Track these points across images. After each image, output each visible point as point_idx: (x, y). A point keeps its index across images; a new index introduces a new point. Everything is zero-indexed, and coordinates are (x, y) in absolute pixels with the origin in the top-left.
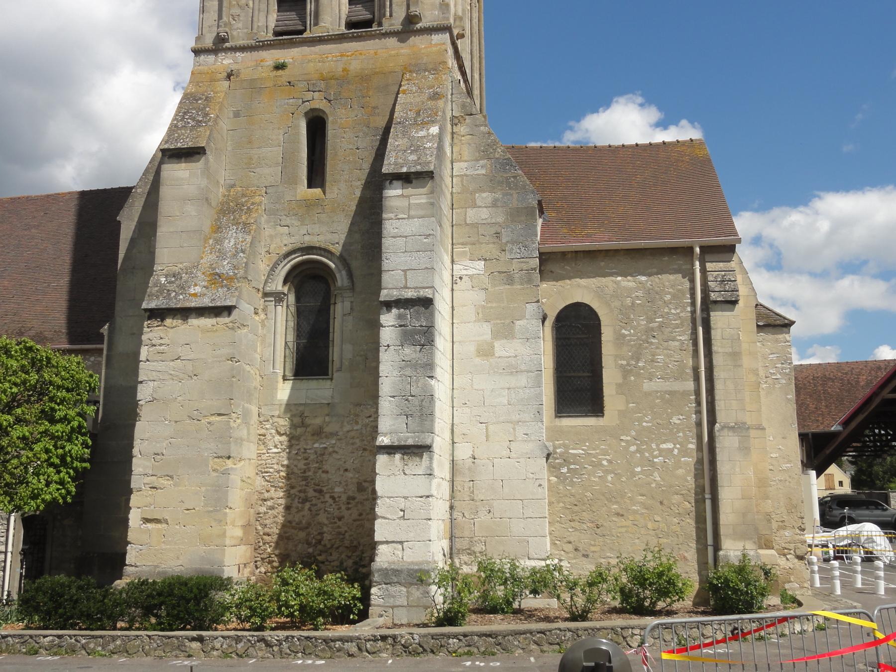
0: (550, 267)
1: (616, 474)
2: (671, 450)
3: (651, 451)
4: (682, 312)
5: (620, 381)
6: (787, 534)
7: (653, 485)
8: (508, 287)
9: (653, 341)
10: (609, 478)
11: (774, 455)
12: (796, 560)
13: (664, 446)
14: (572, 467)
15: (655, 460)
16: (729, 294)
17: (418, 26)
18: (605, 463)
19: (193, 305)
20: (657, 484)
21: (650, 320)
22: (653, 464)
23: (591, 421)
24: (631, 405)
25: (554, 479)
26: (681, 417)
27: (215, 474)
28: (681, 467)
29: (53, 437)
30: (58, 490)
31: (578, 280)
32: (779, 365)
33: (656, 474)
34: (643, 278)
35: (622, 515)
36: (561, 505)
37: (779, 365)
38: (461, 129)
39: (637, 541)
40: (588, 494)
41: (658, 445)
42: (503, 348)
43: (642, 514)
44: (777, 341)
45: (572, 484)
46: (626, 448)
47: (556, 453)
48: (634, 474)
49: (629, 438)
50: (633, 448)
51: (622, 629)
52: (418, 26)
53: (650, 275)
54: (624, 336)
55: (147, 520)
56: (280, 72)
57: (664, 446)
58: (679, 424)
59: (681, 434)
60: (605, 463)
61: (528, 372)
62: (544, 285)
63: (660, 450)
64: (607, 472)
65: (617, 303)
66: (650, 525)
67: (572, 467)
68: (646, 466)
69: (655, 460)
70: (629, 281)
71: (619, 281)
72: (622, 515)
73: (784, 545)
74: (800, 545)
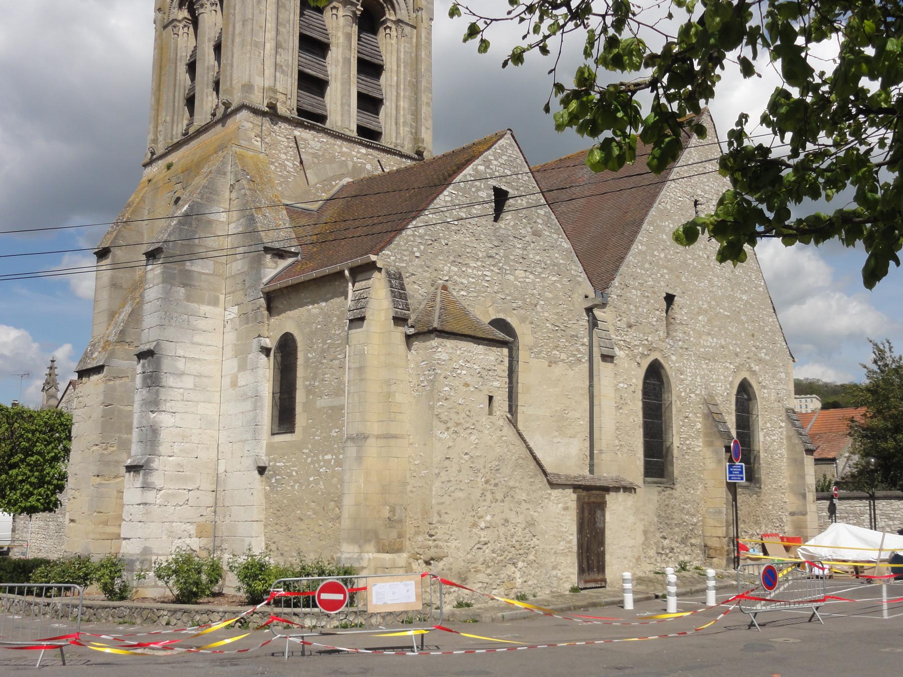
0: (277, 304)
1: (300, 483)
2: (330, 461)
3: (318, 461)
4: (342, 332)
5: (305, 401)
6: (420, 539)
7: (320, 493)
8: (246, 326)
9: (324, 361)
10: (296, 487)
11: (417, 462)
12: (424, 565)
13: (327, 457)
14: (277, 477)
15: (321, 470)
16: (358, 311)
17: (229, 110)
18: (294, 473)
19: (90, 366)
20: (322, 492)
21: (324, 343)
22: (319, 474)
23: (287, 437)
24: (310, 421)
25: (268, 488)
26: (337, 430)
27: (92, 488)
28: (335, 477)
29: (28, 465)
30: (38, 500)
31: (289, 312)
32: (426, 373)
33: (321, 483)
34: (324, 304)
35: (302, 520)
36: (272, 510)
37: (426, 373)
38: (234, 195)
39: (309, 542)
40: (285, 501)
41: (323, 457)
42: (244, 379)
43: (312, 519)
44: (426, 348)
45: (277, 493)
46: (306, 460)
47: (269, 466)
48: (309, 483)
49: (307, 451)
50: (309, 460)
51: (157, 610)
52: (232, 108)
53: (326, 300)
54: (310, 358)
55: (72, 521)
56: (172, 168)
57: (327, 457)
58: (336, 437)
59: (336, 446)
60: (294, 473)
61: (253, 397)
62: (272, 320)
63: (324, 461)
64: (296, 481)
65: (308, 330)
66: (317, 529)
67: (277, 477)
68: (316, 476)
69: (321, 470)
70: (315, 308)
71: (310, 310)
72: (302, 520)
73: (416, 550)
74: (426, 550)
